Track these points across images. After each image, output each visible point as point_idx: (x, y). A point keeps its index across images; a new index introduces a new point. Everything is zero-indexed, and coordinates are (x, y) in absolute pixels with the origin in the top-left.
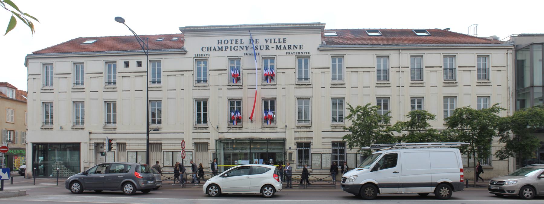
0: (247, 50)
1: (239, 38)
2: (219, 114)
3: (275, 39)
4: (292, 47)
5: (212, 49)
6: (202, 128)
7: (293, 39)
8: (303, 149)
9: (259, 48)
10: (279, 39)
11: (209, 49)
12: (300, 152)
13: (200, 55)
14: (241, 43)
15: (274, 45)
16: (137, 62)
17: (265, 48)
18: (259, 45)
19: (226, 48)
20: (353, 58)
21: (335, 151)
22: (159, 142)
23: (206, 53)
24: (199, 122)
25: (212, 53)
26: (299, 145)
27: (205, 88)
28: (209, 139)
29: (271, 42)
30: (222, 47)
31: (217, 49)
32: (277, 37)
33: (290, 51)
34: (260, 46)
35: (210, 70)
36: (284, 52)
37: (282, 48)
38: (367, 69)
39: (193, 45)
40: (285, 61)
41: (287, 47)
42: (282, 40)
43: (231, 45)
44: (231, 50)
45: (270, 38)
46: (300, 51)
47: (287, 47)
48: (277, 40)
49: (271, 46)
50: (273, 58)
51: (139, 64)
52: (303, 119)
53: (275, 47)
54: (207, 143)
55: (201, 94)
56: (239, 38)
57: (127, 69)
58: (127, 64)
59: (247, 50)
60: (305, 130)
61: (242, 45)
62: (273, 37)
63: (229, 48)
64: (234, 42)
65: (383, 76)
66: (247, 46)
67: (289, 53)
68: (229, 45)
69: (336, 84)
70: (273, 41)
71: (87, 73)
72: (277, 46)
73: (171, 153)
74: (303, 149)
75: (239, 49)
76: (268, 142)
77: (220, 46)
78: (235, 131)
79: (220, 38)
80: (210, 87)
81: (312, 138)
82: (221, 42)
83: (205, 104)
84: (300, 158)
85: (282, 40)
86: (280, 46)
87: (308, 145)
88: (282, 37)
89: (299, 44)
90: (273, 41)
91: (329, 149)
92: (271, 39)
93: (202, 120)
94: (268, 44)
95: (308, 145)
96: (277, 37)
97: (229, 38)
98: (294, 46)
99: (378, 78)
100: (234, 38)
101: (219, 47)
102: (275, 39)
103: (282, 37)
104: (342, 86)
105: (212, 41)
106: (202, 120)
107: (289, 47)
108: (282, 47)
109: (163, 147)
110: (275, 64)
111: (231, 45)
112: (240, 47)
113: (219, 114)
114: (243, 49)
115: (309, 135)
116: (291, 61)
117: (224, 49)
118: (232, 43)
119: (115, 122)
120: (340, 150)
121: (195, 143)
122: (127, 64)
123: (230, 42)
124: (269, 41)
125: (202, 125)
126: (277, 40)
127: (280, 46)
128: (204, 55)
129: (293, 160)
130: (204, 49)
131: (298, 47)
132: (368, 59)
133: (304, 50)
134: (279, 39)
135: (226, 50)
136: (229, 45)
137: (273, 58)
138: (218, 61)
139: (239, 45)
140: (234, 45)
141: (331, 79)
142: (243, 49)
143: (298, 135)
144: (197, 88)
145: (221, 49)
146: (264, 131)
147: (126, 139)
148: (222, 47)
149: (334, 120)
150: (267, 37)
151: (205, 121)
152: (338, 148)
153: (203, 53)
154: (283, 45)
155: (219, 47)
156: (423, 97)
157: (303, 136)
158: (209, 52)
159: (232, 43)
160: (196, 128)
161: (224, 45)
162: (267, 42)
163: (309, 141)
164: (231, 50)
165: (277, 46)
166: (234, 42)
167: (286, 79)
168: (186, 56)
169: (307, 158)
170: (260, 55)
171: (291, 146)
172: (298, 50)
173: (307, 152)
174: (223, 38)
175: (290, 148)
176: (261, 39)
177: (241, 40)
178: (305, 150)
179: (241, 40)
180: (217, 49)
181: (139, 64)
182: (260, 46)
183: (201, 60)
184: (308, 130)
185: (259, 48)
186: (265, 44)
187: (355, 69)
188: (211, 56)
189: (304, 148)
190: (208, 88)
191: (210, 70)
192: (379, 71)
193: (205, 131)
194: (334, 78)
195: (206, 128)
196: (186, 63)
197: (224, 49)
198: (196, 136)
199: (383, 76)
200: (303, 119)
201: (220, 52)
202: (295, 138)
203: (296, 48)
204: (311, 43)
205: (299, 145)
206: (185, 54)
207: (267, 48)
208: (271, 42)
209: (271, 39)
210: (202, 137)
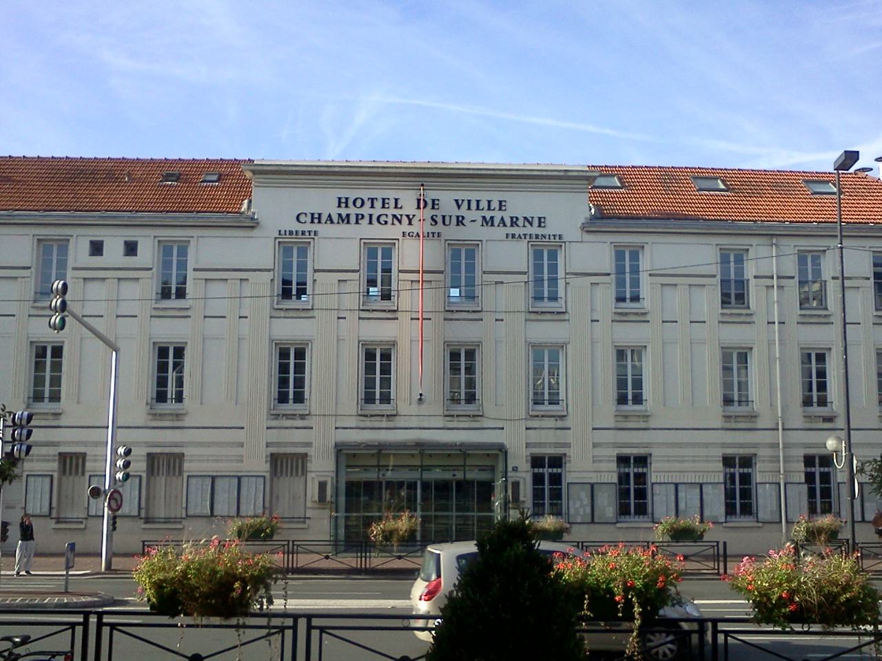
0: (410, 223)
1: (391, 195)
2: (333, 378)
3: (478, 202)
4: (520, 222)
5: (324, 219)
6: (287, 416)
7: (521, 203)
8: (546, 471)
9: (439, 220)
10: (489, 202)
11: (316, 218)
12: (538, 480)
13: (291, 233)
14: (396, 207)
15: (478, 215)
16: (92, 243)
17: (454, 220)
18: (439, 213)
19: (359, 218)
20: (663, 253)
21: (624, 478)
22: (176, 450)
23: (308, 227)
24: (283, 398)
25: (324, 229)
26: (537, 461)
27: (302, 314)
28: (309, 445)
29: (469, 208)
30: (348, 215)
31: (335, 218)
32: (484, 197)
33: (516, 230)
34: (444, 217)
35: (315, 271)
36: (500, 232)
37: (496, 223)
38: (695, 279)
39: (274, 208)
40: (505, 254)
41: (508, 222)
42: (495, 205)
43: (372, 211)
44: (371, 223)
45: (466, 198)
46: (540, 231)
47: (508, 222)
48: (484, 204)
49: (469, 215)
50: (472, 250)
51: (131, 249)
52: (546, 397)
53: (480, 220)
54: (304, 456)
55: (291, 330)
56: (391, 195)
57: (97, 261)
58: (97, 248)
59: (410, 223)
60: (551, 423)
61: (397, 212)
62: (474, 196)
63: (367, 218)
64: (378, 204)
65: (734, 295)
66: (411, 214)
67: (513, 236)
68: (366, 210)
69: (626, 314)
70: (474, 205)
71: (74, 269)
72: (484, 218)
73: (209, 481)
74: (546, 471)
75: (390, 220)
76: (463, 452)
77: (344, 212)
78: (377, 424)
79: (344, 193)
80: (315, 313)
81: (568, 445)
82: (346, 203)
83: (300, 354)
84: (538, 495)
85: (495, 205)
86: (492, 218)
87: (557, 461)
88: (496, 197)
89: (536, 215)
90: (474, 205)
91: (609, 474)
92: (469, 201)
93: (291, 396)
94: (463, 211)
95: (557, 461)
96: (484, 197)
97: (365, 194)
98: (525, 218)
99: (725, 301)
100: (379, 194)
101: (340, 215)
102: (478, 202)
103: (496, 197)
104: (642, 318)
105: (324, 200)
106: (291, 396)
107: (514, 221)
108: (497, 221)
109: (186, 466)
110: (477, 260)
111: (372, 211)
112: (394, 216)
113: (333, 378)
114: (400, 221)
115: (561, 436)
116: (517, 256)
117: (353, 219)
118: (372, 207)
119: (55, 397)
120: (636, 475)
121: (272, 455)
122: (97, 248)
123: (368, 204)
124: (465, 204)
125: (291, 407)
126: (484, 204)
127: (492, 218)
128: (303, 233)
129: (522, 498)
130: (302, 218)
131: (536, 222)
132: (699, 254)
133: (548, 230)
134: (489, 202)
135: (357, 223)
136: (366, 210)
137: (472, 250)
138: (338, 249)
139: (391, 211)
140: (377, 211)
141: (614, 301)
142: (400, 221)
143: (534, 436)
144: (282, 314)
145: (345, 219)
146: (450, 425)
147: (85, 444)
148: (348, 215)
149: (622, 400)
150: (460, 195)
151: (299, 398)
152: (632, 470)
153: (301, 227)
154: (498, 215)
155: (340, 215)
156: (830, 349)
157: (547, 440)
158: (314, 227)
159: (372, 207)
160: (277, 417)
161: (353, 211)
162: (459, 207)
163: (561, 451)
164: (371, 223)
165: (484, 218)
166: (378, 204)
167: (507, 298)
168: (255, 233)
169: (556, 495)
170: (442, 239)
171: (520, 462)
172: (535, 230)
173: (556, 479)
174: (352, 194)
175: (515, 469)
176: (447, 198)
177: (396, 200)
178: (551, 475)
179: (396, 200)
180: (335, 218)
181: (131, 249)
182: (444, 217)
183: (293, 247)
184: (560, 424)
185: (439, 220)
186: (456, 212)
187: (668, 279)
188: (320, 235)
189: (549, 471)
190: (311, 314)
191: (315, 271)
192: (725, 282)
193: (299, 423)
194: (621, 299)
195: (303, 417)
196: (257, 251)
197: (353, 219)
198: (273, 436)
199: (734, 295)
200: (546, 397)
201: (344, 227)
202: (528, 445)
203: (531, 224)
204: (567, 213)
205: (537, 461)
206: (252, 227)
207: (460, 221)
208: (469, 208)
209: (469, 201)
210: (291, 438)
